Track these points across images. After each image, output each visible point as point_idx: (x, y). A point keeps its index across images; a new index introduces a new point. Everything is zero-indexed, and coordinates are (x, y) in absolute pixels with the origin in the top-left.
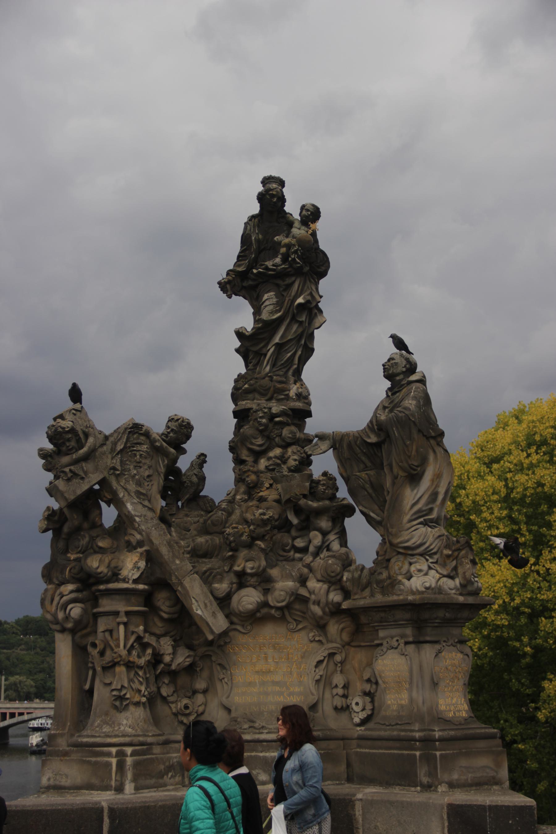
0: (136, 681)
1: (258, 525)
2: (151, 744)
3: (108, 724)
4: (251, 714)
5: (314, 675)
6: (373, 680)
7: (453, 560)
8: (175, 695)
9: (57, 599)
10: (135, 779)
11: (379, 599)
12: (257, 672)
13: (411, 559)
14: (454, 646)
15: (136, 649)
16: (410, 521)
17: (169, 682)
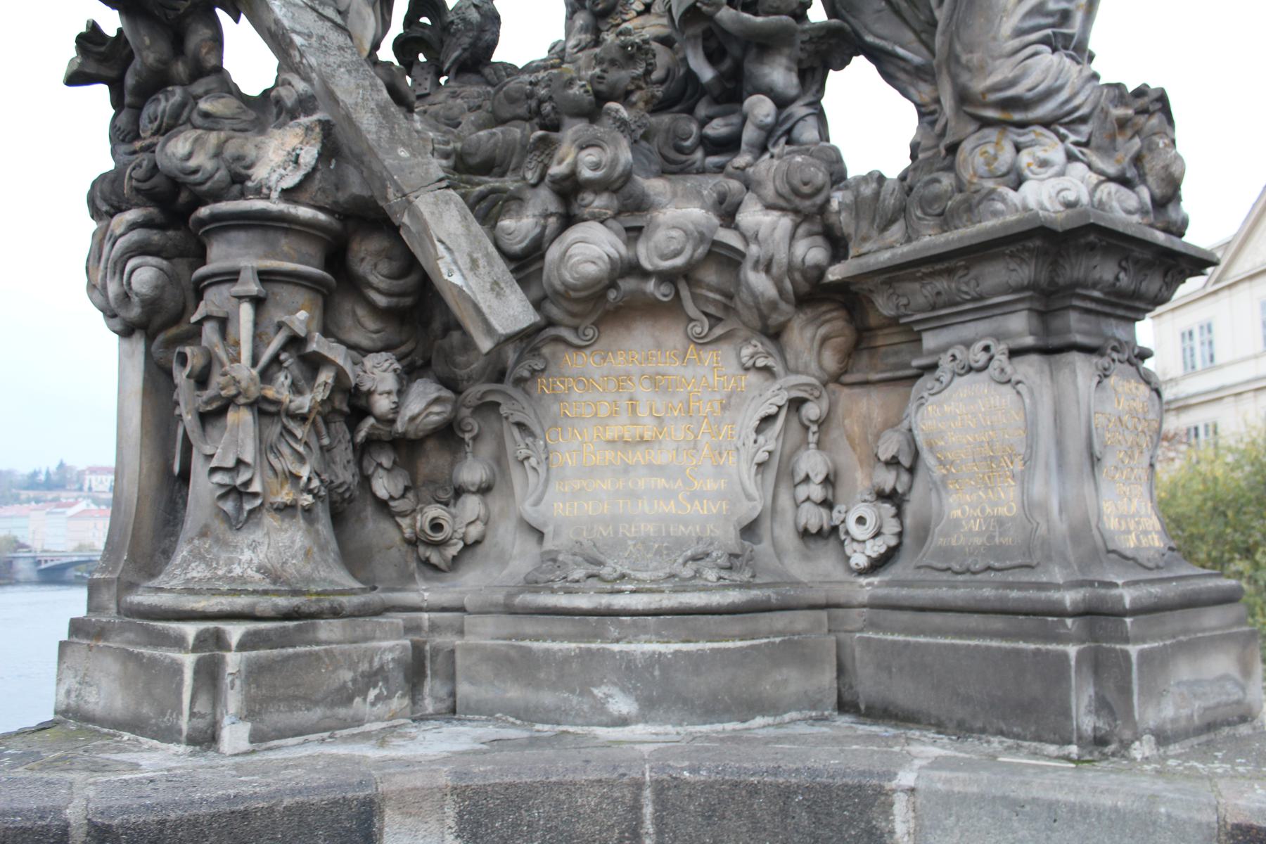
0: (286, 450)
1: (613, 63)
3: (202, 558)
4: (595, 545)
5: (754, 450)
6: (905, 461)
7: (1132, 137)
8: (410, 495)
10: (250, 712)
11: (931, 240)
12: (612, 442)
13: (1020, 135)
14: (1131, 364)
15: (287, 368)
16: (1019, 32)
17: (394, 462)
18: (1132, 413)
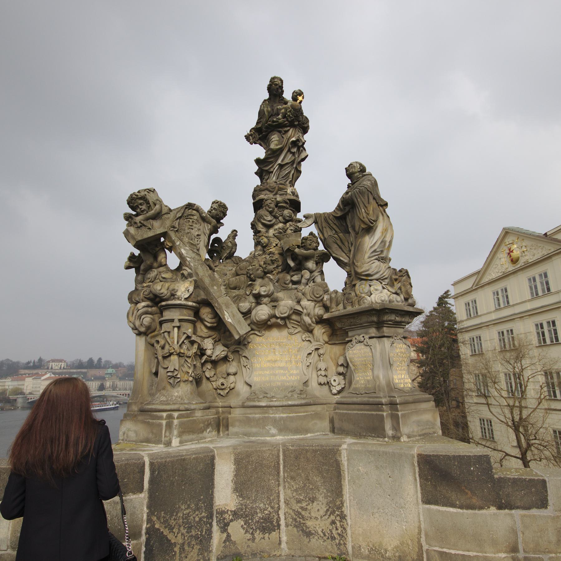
0: (185, 366)
2: (194, 409)
3: (164, 395)
6: (345, 365)
9: (135, 312)
10: (180, 435)
12: (269, 361)
16: (369, 257)
18: (401, 352)
